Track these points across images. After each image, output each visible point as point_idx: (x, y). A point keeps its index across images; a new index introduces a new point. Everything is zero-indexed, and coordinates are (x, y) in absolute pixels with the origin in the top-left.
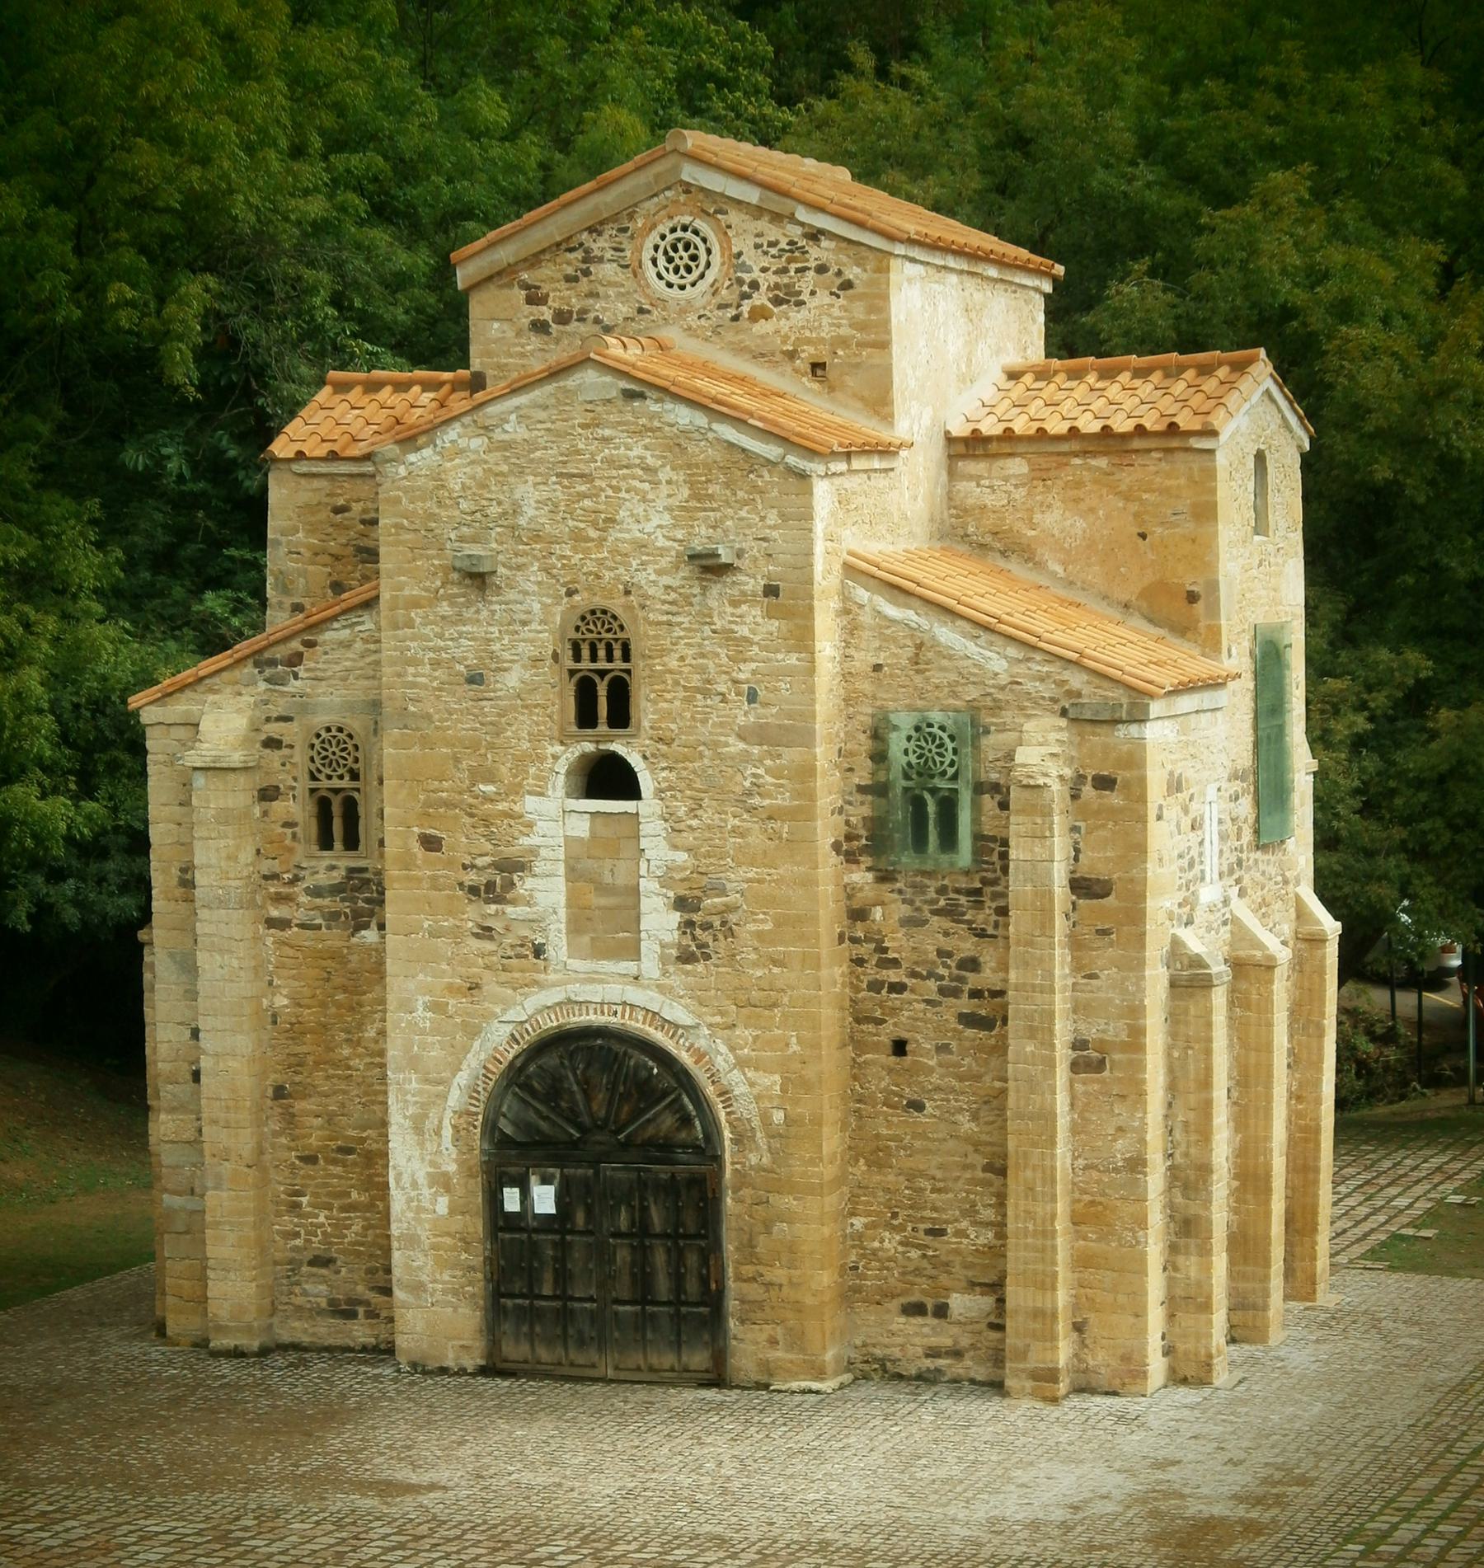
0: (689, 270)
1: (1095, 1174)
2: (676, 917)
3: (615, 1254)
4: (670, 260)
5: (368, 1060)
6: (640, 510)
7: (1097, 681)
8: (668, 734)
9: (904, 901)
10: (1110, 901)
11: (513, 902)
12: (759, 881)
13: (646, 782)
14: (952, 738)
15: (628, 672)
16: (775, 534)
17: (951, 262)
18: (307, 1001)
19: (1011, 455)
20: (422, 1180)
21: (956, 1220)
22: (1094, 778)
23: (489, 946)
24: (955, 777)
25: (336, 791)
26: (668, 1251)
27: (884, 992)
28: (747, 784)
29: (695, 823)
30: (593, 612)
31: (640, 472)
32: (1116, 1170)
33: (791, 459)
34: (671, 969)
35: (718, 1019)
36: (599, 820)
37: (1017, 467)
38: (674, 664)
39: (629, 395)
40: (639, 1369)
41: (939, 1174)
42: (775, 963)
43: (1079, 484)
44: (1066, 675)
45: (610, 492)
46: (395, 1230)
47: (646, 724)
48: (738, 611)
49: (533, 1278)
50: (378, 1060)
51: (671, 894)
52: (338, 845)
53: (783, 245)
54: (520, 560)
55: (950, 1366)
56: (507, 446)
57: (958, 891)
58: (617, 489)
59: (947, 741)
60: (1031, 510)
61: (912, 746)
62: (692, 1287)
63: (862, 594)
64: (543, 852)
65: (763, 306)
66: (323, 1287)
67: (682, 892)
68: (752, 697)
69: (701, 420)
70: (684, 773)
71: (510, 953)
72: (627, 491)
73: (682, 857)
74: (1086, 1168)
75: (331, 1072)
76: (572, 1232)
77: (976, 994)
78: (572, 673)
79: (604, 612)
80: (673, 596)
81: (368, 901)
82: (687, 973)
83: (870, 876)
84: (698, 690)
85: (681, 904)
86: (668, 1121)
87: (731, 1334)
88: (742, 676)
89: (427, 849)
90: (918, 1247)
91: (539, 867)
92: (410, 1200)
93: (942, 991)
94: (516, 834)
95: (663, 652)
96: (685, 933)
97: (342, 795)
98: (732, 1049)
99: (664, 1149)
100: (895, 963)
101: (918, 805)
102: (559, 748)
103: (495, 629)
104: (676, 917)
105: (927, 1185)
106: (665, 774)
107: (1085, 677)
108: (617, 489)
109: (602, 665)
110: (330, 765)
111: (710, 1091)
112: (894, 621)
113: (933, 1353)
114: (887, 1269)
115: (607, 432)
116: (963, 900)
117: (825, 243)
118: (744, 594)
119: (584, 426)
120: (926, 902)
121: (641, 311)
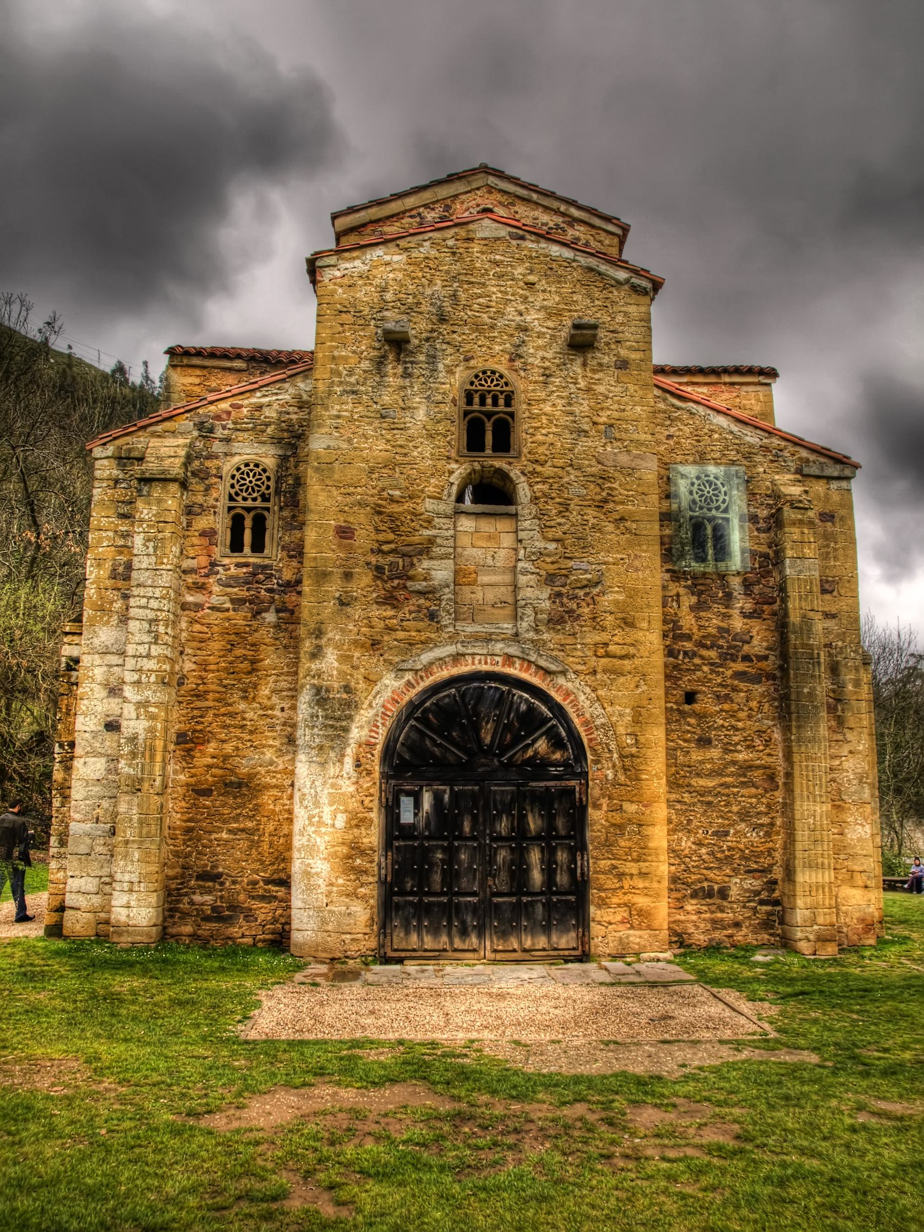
3: (495, 855)
5: (261, 712)
6: (522, 307)
8: (543, 457)
11: (410, 578)
13: (524, 491)
14: (723, 485)
15: (512, 415)
18: (212, 667)
24: (726, 510)
25: (248, 510)
26: (542, 851)
27: (681, 657)
28: (604, 494)
30: (484, 372)
33: (633, 280)
38: (548, 408)
40: (514, 951)
47: (525, 451)
48: (597, 376)
49: (423, 878)
50: (270, 712)
51: (543, 573)
52: (247, 550)
61: (695, 488)
62: (562, 879)
64: (439, 541)
66: (208, 898)
67: (551, 568)
69: (568, 254)
72: (513, 295)
73: (552, 546)
75: (228, 721)
76: (461, 838)
77: (747, 658)
79: (493, 372)
80: (547, 364)
81: (268, 591)
85: (550, 579)
86: (542, 745)
87: (592, 915)
88: (601, 420)
89: (341, 537)
91: (437, 551)
92: (310, 818)
93: (720, 656)
94: (418, 527)
96: (554, 602)
97: (252, 514)
99: (540, 766)
100: (689, 637)
102: (454, 466)
106: (540, 486)
109: (489, 408)
110: (247, 490)
111: (576, 721)
112: (678, 408)
115: (498, 257)
117: (577, 227)
118: (600, 365)
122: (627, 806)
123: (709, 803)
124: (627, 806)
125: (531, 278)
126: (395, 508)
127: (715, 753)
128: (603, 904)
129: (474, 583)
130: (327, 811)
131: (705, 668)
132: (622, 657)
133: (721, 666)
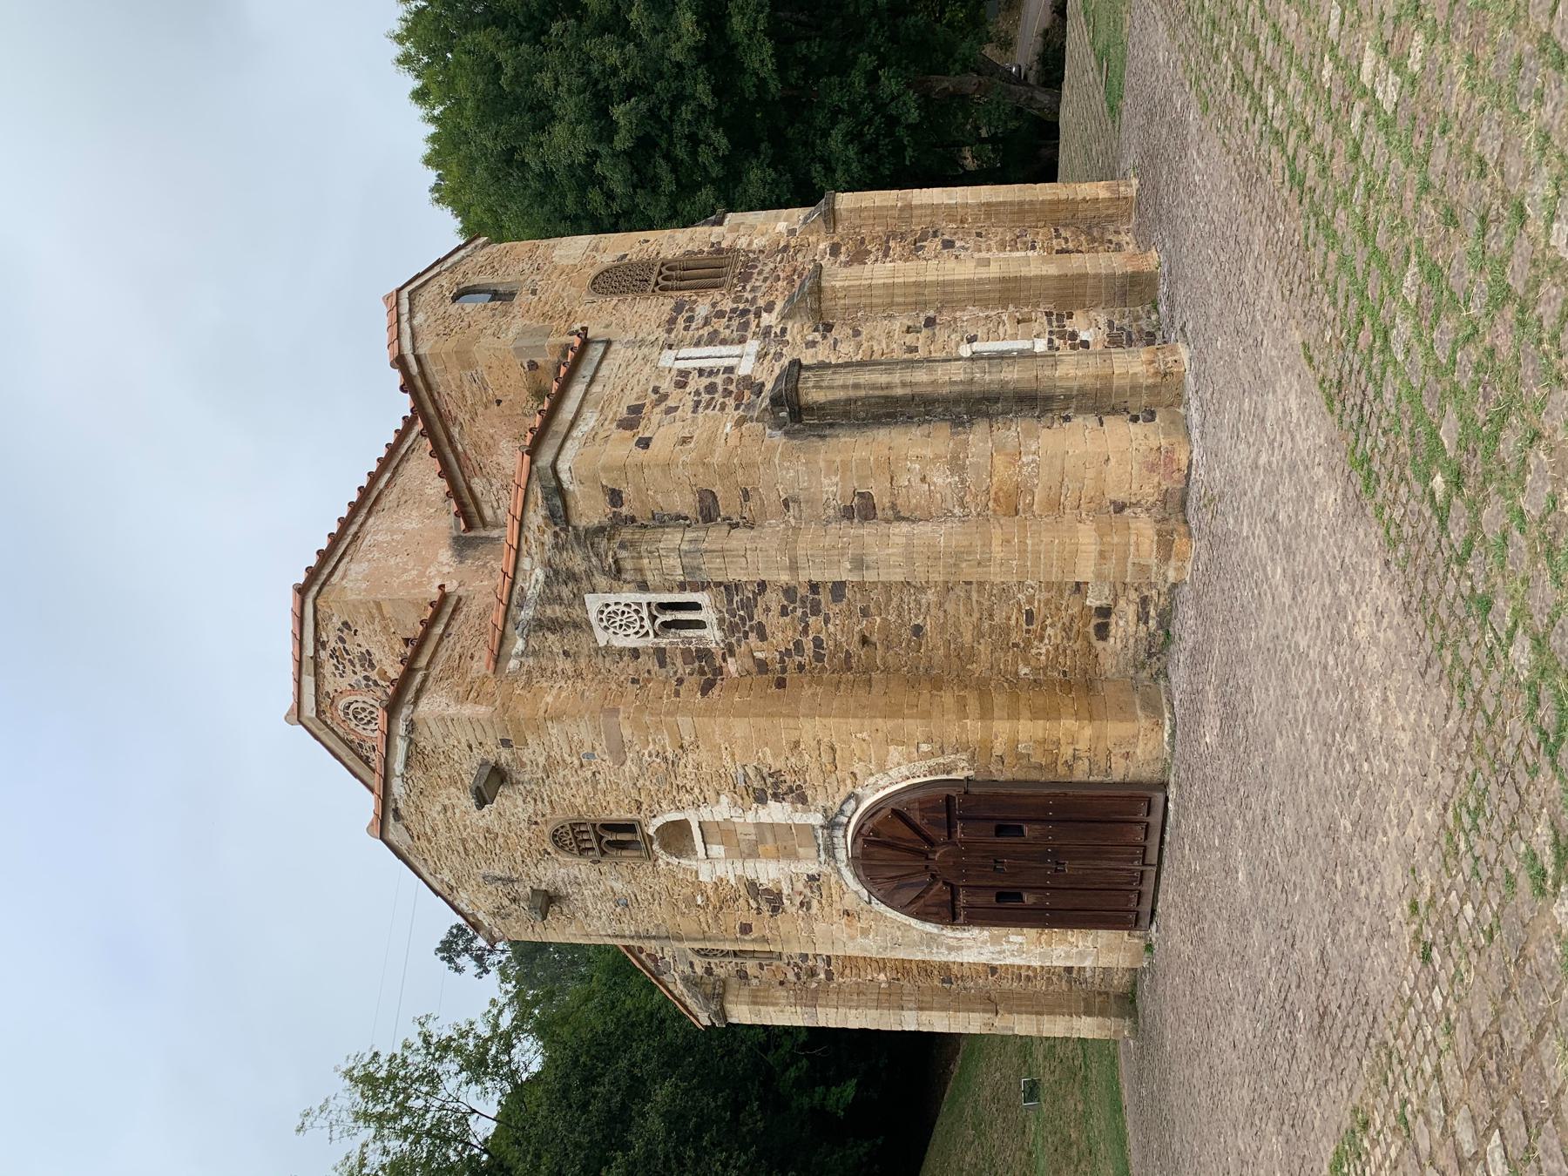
0: (371, 713)
1: (967, 499)
2: (771, 803)
4: (369, 722)
7: (531, 507)
9: (746, 637)
10: (718, 489)
12: (733, 755)
13: (675, 816)
14: (608, 605)
16: (463, 740)
17: (354, 528)
19: (470, 489)
20: (998, 948)
21: (1018, 602)
22: (614, 506)
23: (815, 903)
24: (640, 604)
29: (697, 791)
30: (556, 842)
31: (449, 814)
32: (963, 481)
34: (813, 808)
35: (849, 782)
36: (707, 840)
37: (478, 485)
39: (398, 816)
41: (976, 615)
42: (797, 744)
43: (475, 445)
44: (533, 527)
45: (469, 830)
46: (1036, 963)
47: (629, 816)
51: (755, 805)
54: (533, 878)
55: (1156, 605)
56: (458, 880)
57: (730, 601)
58: (465, 827)
59: (610, 609)
60: (506, 475)
63: (513, 664)
64: (739, 872)
65: (379, 674)
68: (590, 756)
70: (661, 795)
71: (818, 894)
73: (723, 798)
74: (962, 505)
78: (603, 853)
79: (554, 836)
82: (814, 800)
83: (729, 660)
84: (594, 787)
85: (761, 799)
88: (576, 762)
90: (1044, 629)
91: (751, 875)
92: (1013, 955)
95: (573, 806)
98: (872, 775)
100: (798, 644)
101: (667, 625)
103: (586, 892)
104: (771, 803)
105: (986, 625)
107: (530, 514)
108: (465, 827)
109: (592, 836)
113: (1143, 617)
114: (1064, 651)
115: (428, 830)
116: (736, 599)
119: (429, 841)
120: (744, 624)
122: (998, 751)
124: (998, 751)
128: (1107, 772)
130: (1006, 946)
131: (831, 628)
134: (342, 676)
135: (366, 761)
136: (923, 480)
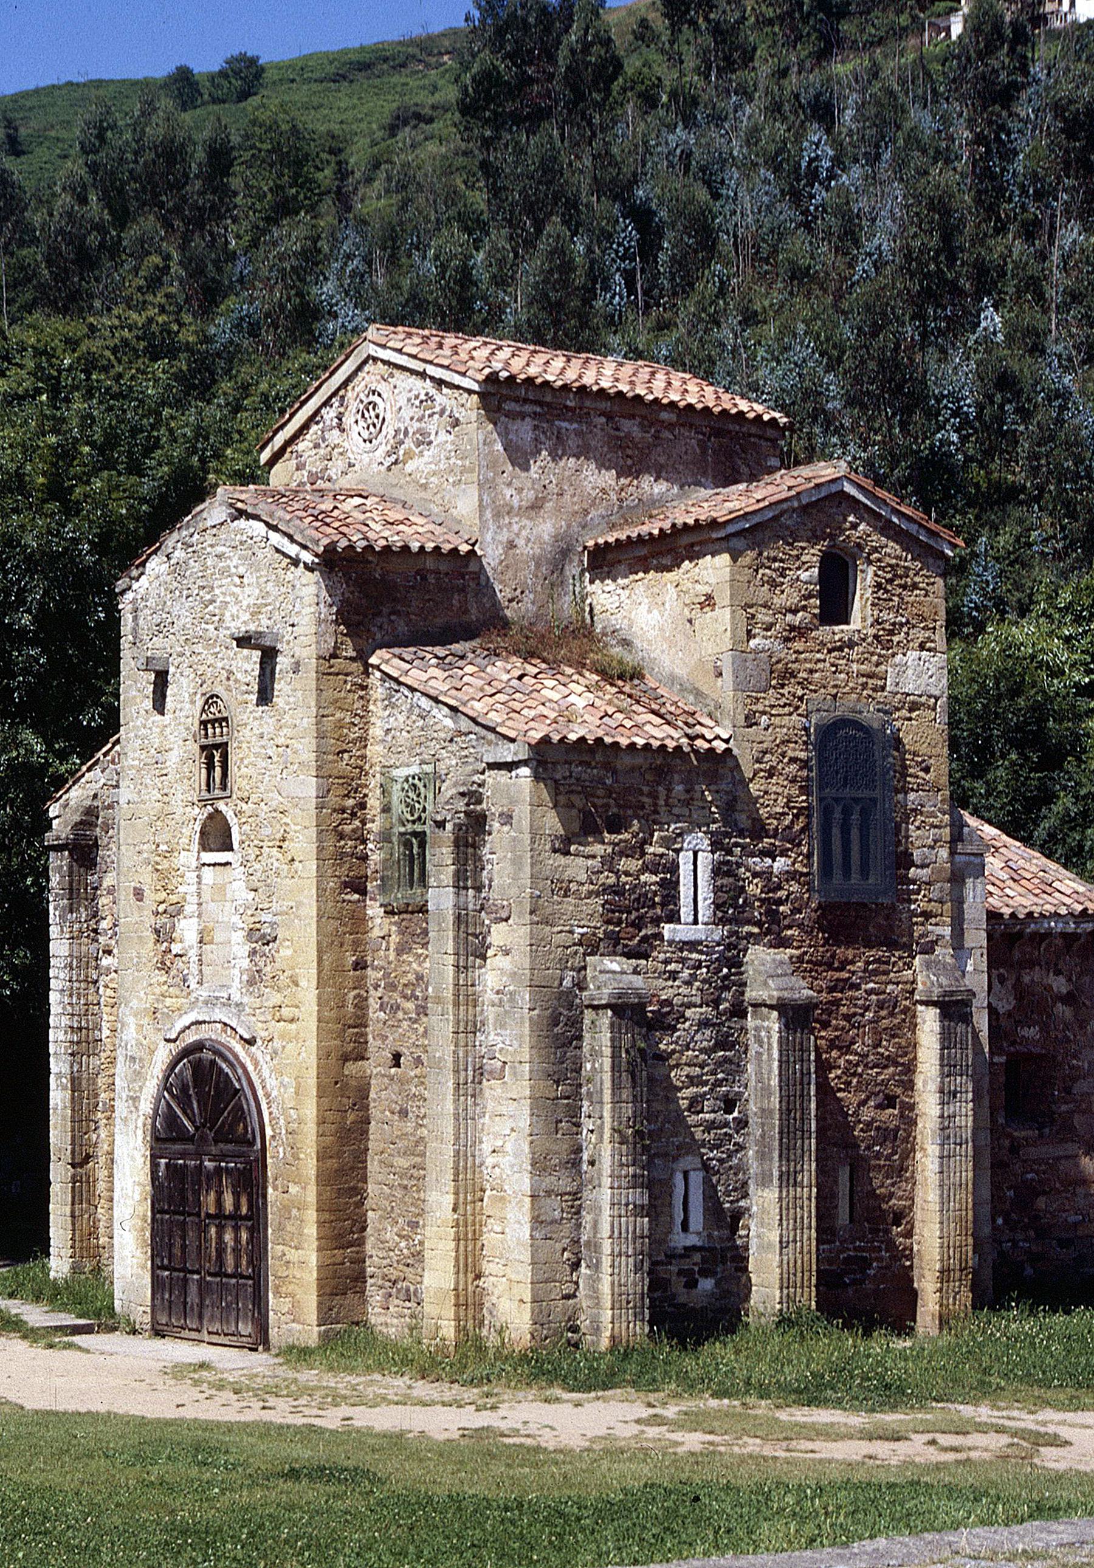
0: (374, 425)
2: (247, 948)
11: (172, 940)
19: (620, 562)
40: (217, 1333)
53: (422, 397)
109: (219, 740)
121: (351, 465)
123: (405, 1187)
125: (242, 570)
126: (165, 865)
127: (410, 1126)
129: (211, 942)
131: (405, 1024)
132: (292, 1021)
133: (415, 1021)
134: (409, 400)
135: (327, 403)
136: (513, 1130)
